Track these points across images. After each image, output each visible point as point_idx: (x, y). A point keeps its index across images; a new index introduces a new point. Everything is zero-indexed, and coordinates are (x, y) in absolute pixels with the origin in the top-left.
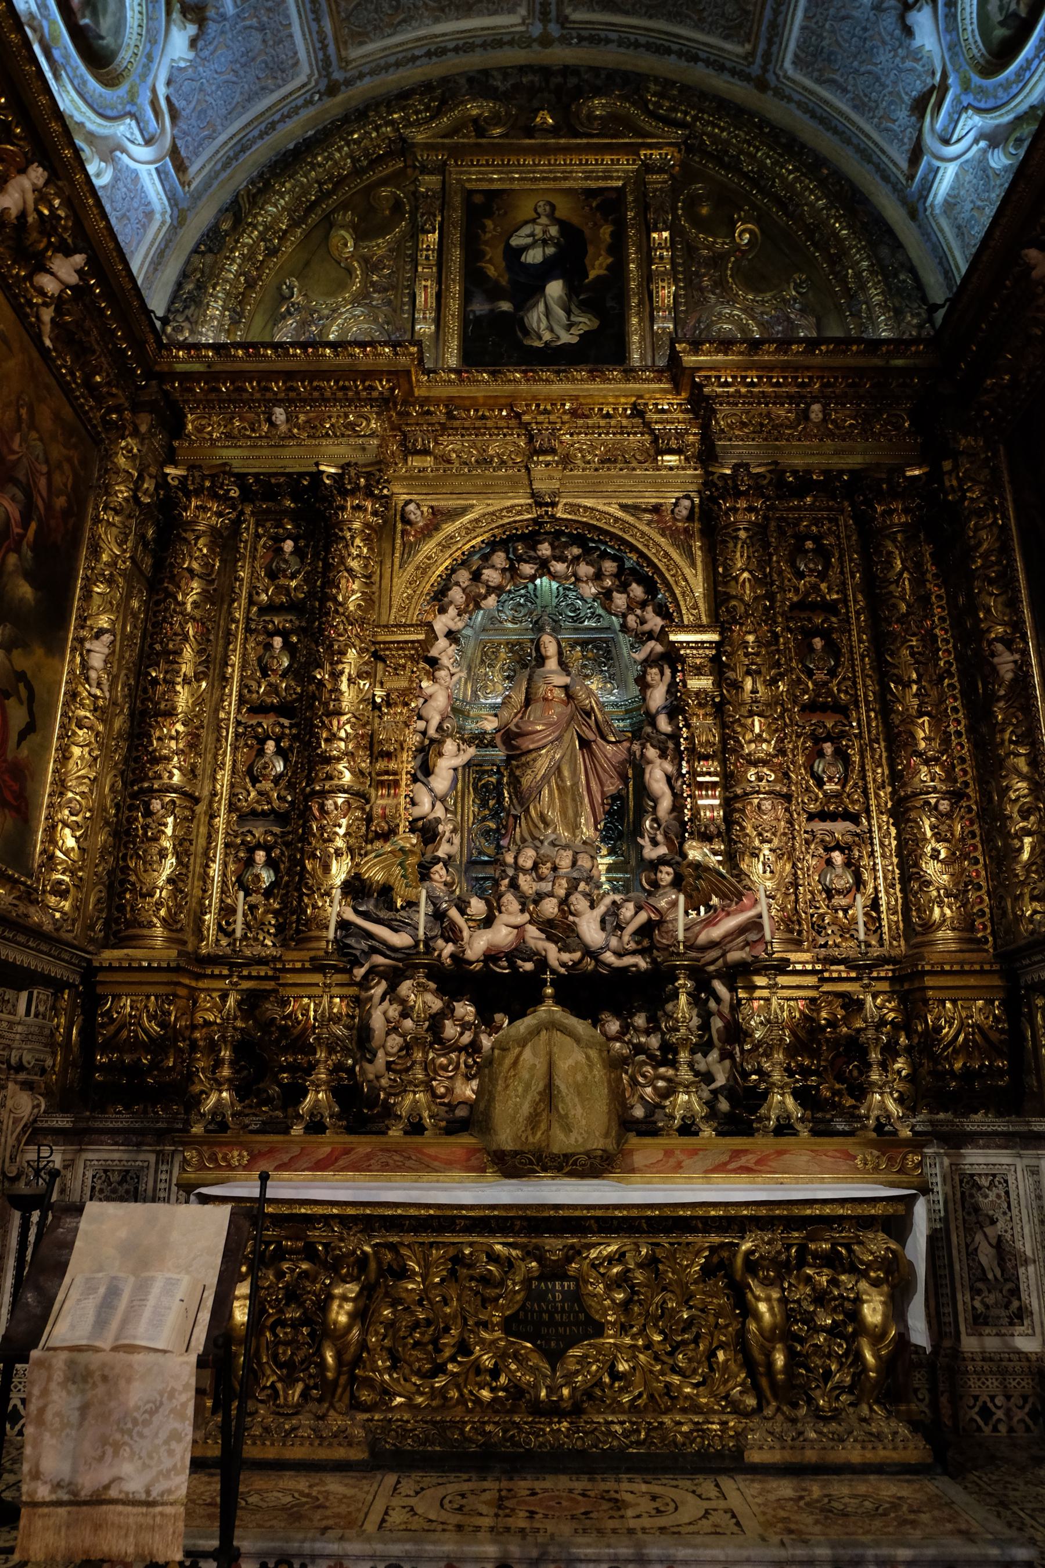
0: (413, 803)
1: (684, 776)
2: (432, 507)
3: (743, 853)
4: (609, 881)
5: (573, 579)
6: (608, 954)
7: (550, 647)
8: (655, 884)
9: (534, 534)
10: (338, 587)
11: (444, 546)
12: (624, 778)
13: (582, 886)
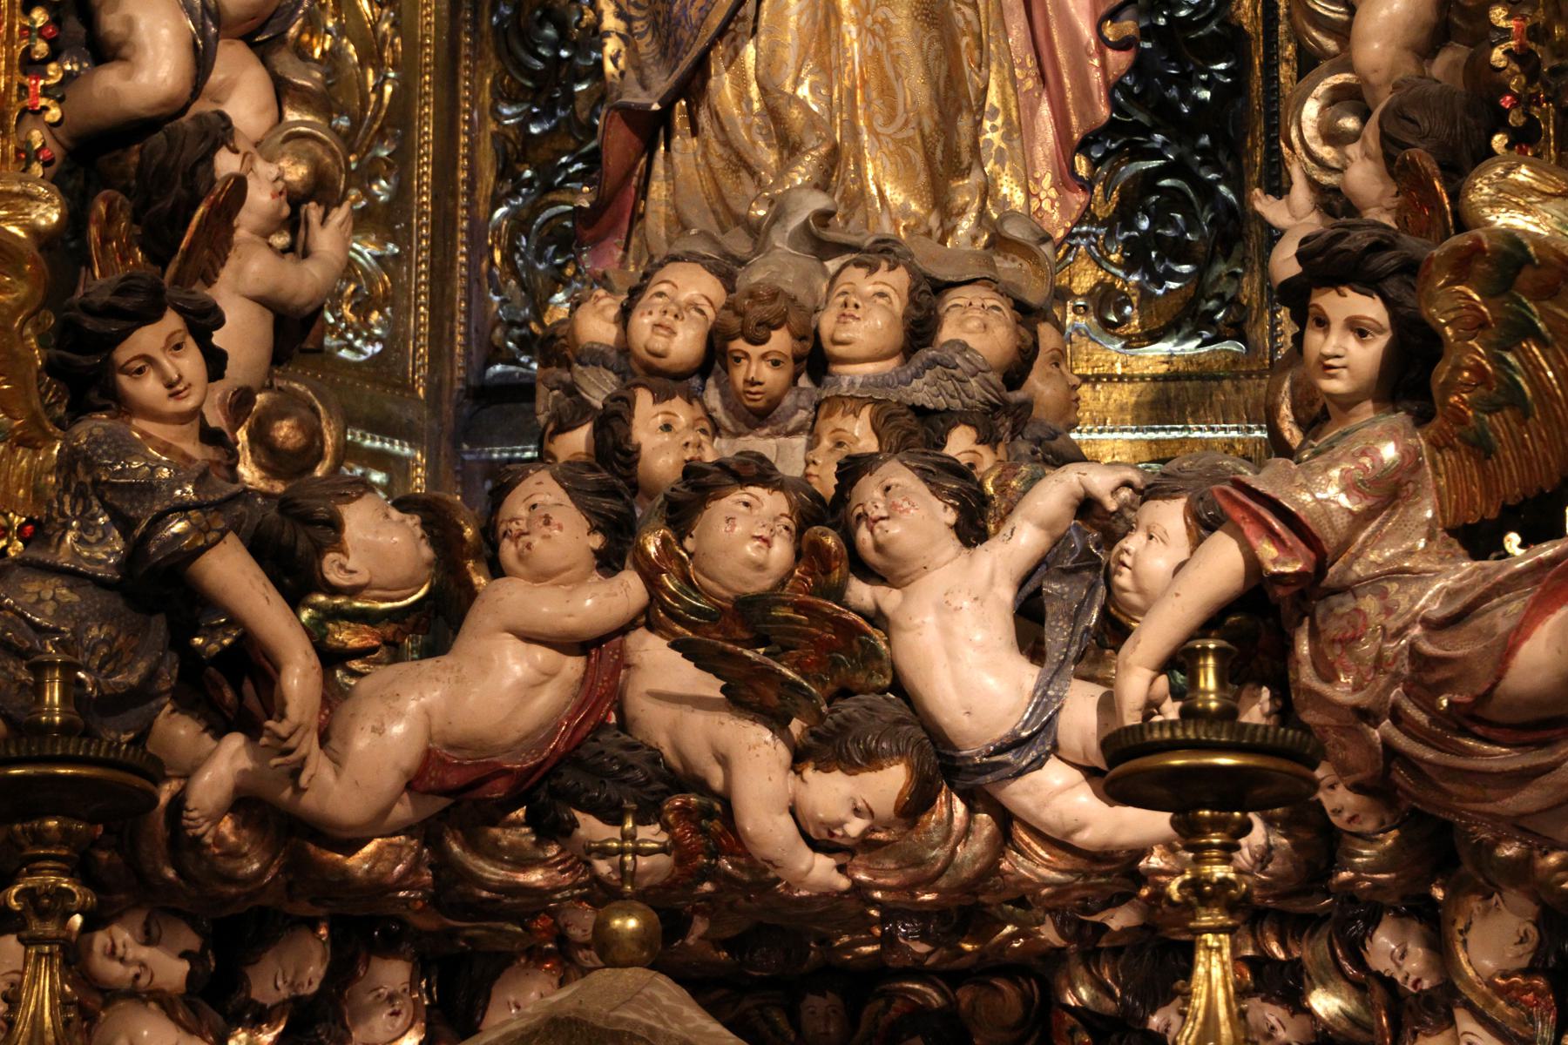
6: (1056, 774)
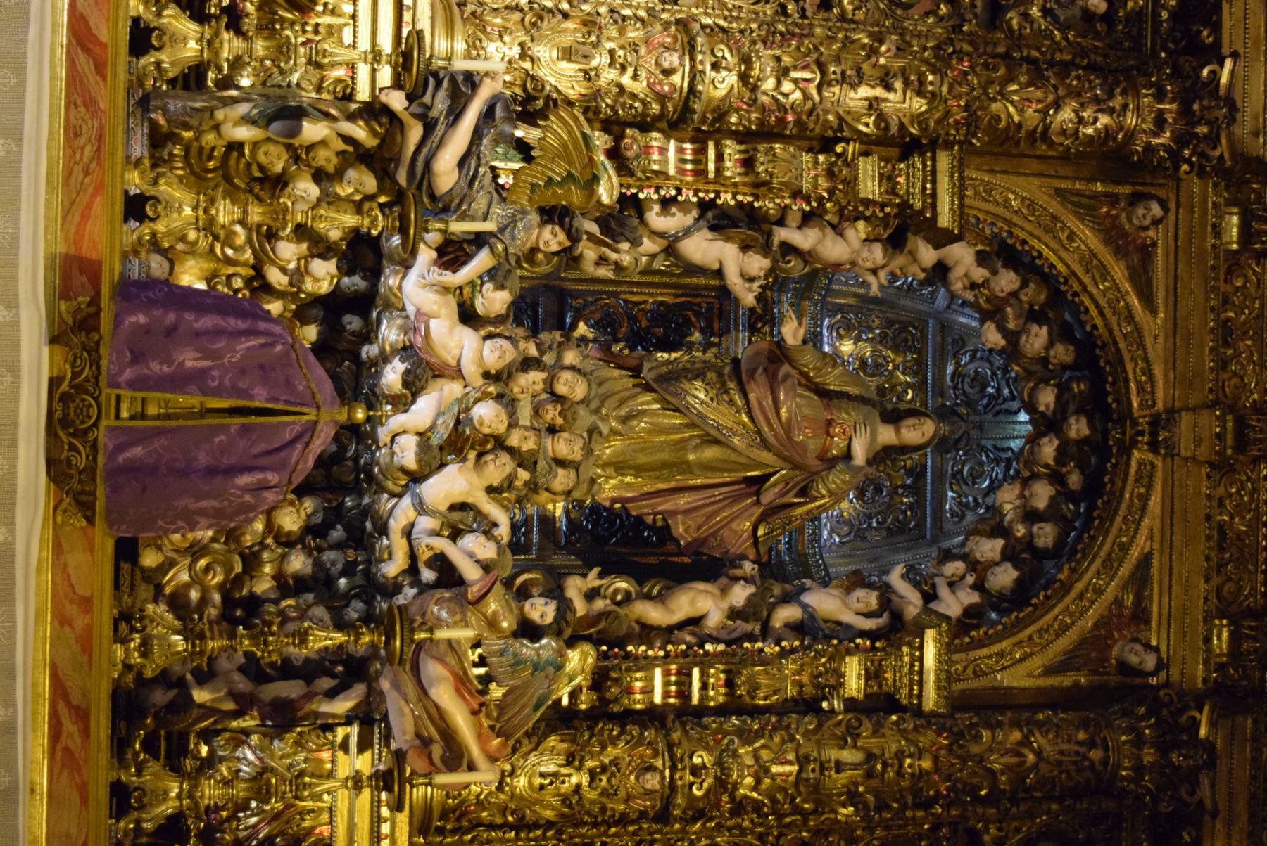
0: (666, 203)
1: (701, 646)
2: (1154, 244)
3: (573, 741)
4: (527, 521)
5: (1026, 474)
6: (412, 514)
7: (917, 432)
8: (523, 594)
9: (1105, 410)
10: (1029, 84)
11: (1089, 261)
12: (697, 547)
13: (524, 475)
